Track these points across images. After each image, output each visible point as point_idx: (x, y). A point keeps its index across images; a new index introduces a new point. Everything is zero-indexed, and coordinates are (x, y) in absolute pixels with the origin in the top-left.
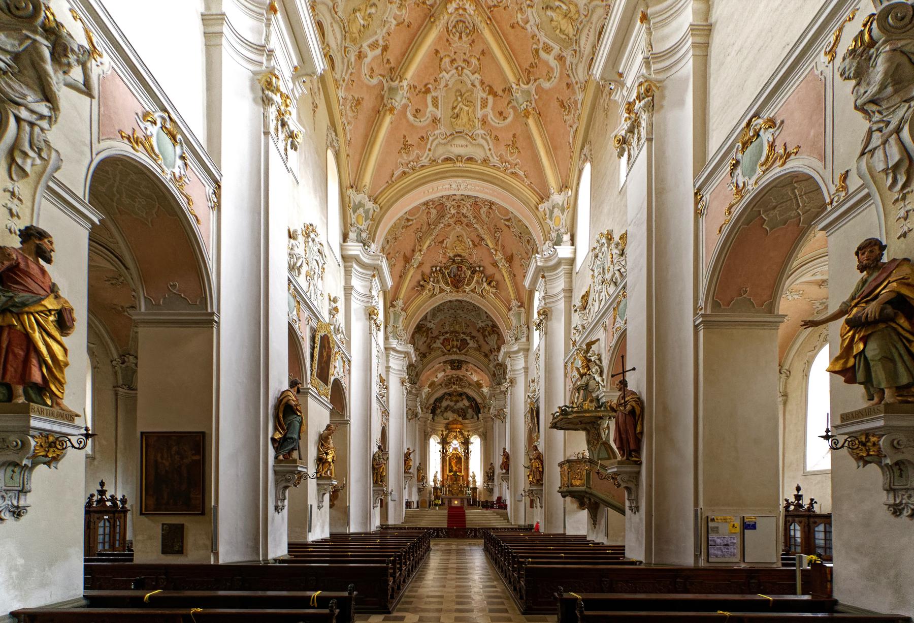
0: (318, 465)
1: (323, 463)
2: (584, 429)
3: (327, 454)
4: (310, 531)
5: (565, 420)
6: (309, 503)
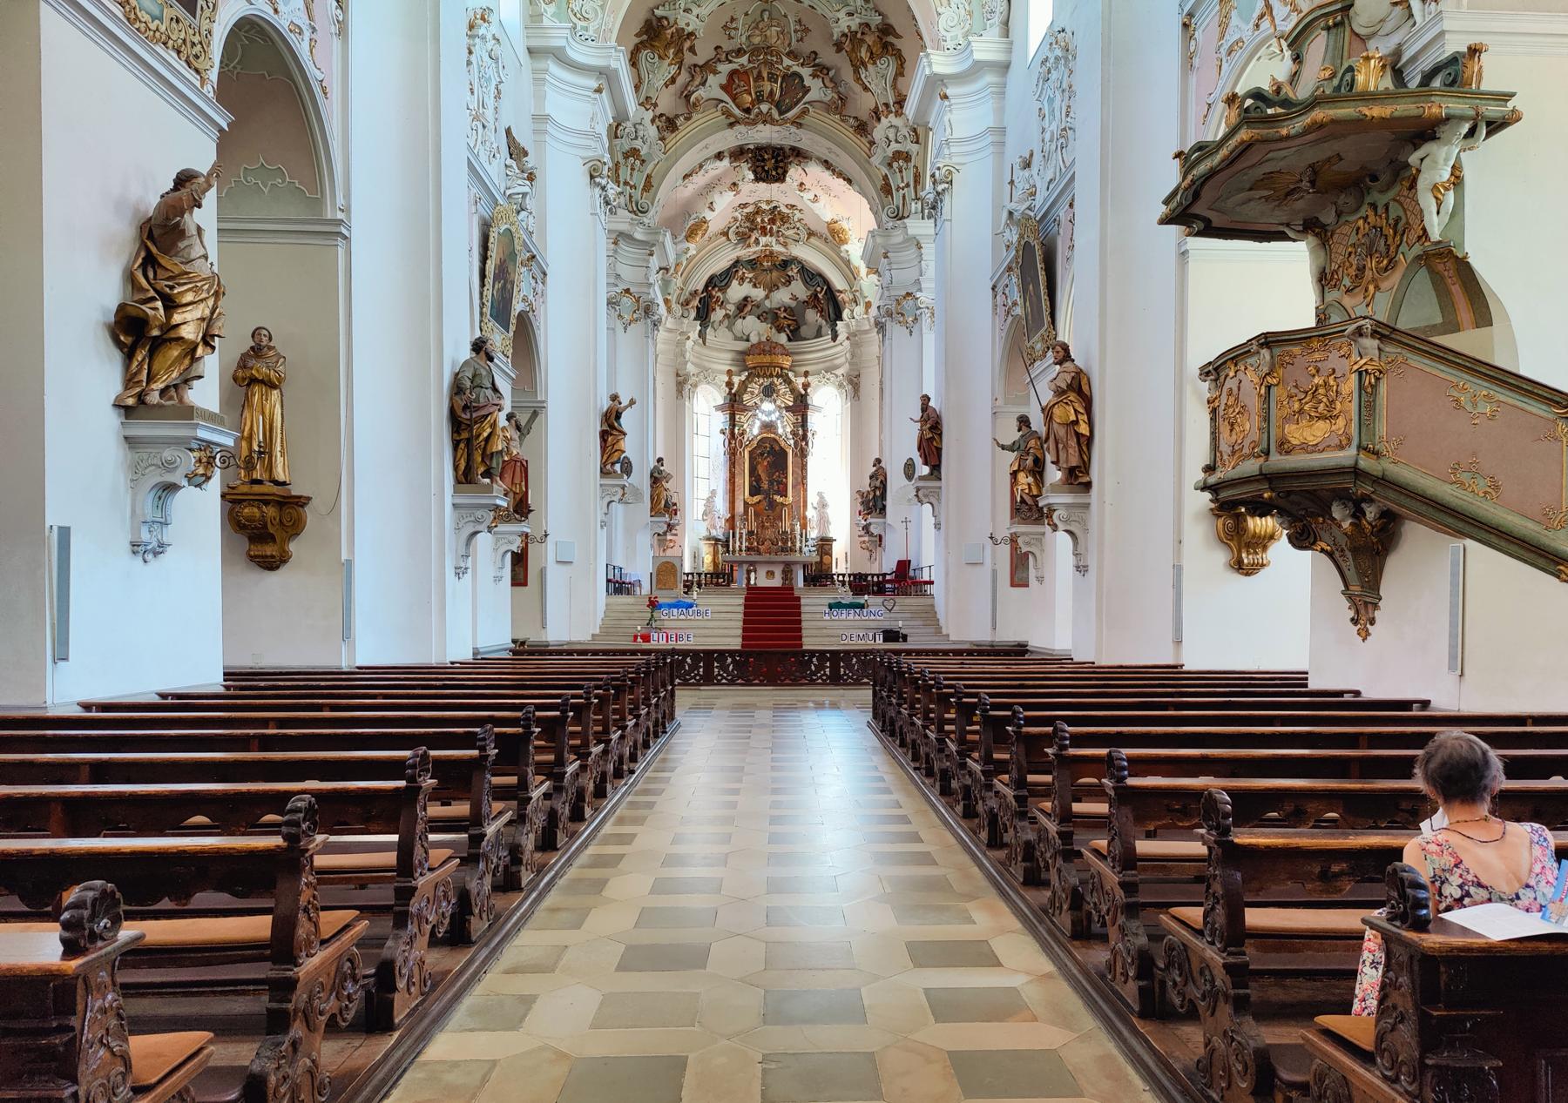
0: (129, 355)
1: (157, 345)
2: (1312, 227)
3: (171, 305)
4: (62, 655)
5: (1217, 198)
6: (53, 518)
